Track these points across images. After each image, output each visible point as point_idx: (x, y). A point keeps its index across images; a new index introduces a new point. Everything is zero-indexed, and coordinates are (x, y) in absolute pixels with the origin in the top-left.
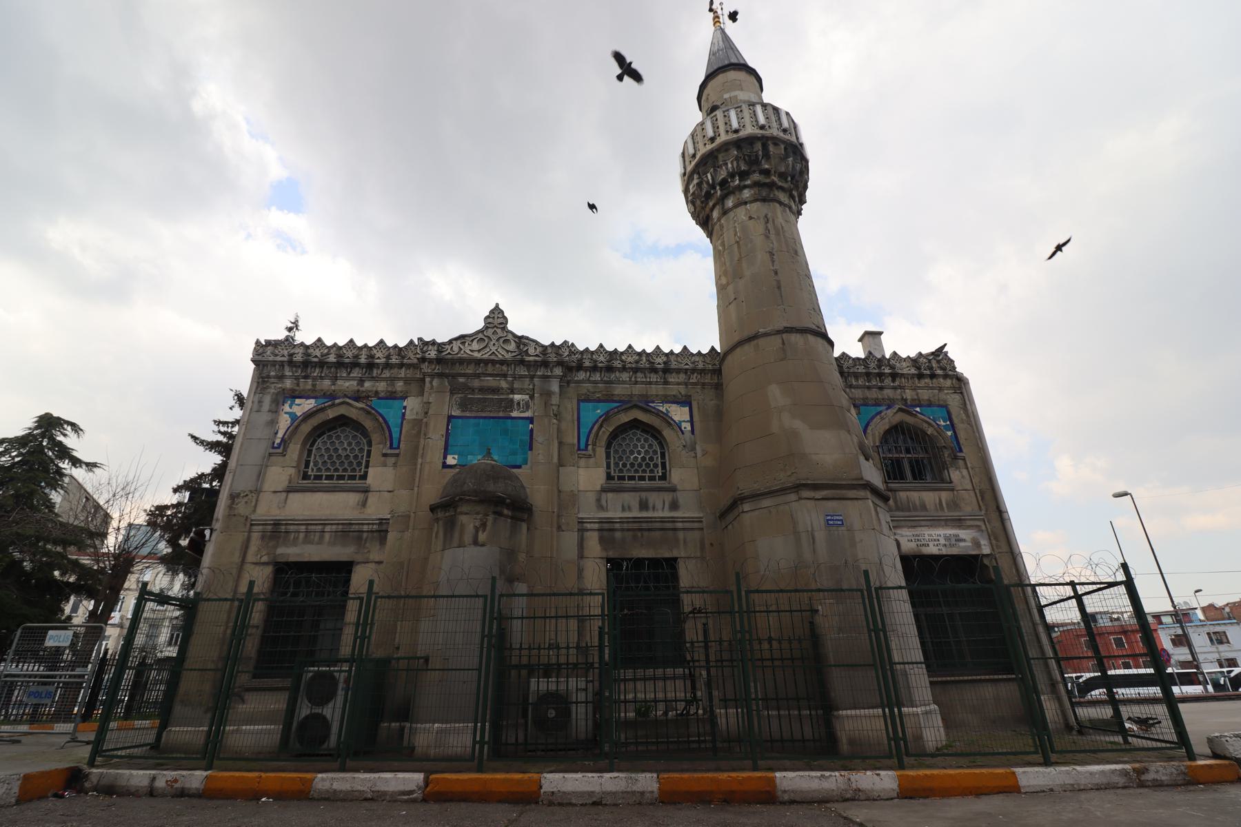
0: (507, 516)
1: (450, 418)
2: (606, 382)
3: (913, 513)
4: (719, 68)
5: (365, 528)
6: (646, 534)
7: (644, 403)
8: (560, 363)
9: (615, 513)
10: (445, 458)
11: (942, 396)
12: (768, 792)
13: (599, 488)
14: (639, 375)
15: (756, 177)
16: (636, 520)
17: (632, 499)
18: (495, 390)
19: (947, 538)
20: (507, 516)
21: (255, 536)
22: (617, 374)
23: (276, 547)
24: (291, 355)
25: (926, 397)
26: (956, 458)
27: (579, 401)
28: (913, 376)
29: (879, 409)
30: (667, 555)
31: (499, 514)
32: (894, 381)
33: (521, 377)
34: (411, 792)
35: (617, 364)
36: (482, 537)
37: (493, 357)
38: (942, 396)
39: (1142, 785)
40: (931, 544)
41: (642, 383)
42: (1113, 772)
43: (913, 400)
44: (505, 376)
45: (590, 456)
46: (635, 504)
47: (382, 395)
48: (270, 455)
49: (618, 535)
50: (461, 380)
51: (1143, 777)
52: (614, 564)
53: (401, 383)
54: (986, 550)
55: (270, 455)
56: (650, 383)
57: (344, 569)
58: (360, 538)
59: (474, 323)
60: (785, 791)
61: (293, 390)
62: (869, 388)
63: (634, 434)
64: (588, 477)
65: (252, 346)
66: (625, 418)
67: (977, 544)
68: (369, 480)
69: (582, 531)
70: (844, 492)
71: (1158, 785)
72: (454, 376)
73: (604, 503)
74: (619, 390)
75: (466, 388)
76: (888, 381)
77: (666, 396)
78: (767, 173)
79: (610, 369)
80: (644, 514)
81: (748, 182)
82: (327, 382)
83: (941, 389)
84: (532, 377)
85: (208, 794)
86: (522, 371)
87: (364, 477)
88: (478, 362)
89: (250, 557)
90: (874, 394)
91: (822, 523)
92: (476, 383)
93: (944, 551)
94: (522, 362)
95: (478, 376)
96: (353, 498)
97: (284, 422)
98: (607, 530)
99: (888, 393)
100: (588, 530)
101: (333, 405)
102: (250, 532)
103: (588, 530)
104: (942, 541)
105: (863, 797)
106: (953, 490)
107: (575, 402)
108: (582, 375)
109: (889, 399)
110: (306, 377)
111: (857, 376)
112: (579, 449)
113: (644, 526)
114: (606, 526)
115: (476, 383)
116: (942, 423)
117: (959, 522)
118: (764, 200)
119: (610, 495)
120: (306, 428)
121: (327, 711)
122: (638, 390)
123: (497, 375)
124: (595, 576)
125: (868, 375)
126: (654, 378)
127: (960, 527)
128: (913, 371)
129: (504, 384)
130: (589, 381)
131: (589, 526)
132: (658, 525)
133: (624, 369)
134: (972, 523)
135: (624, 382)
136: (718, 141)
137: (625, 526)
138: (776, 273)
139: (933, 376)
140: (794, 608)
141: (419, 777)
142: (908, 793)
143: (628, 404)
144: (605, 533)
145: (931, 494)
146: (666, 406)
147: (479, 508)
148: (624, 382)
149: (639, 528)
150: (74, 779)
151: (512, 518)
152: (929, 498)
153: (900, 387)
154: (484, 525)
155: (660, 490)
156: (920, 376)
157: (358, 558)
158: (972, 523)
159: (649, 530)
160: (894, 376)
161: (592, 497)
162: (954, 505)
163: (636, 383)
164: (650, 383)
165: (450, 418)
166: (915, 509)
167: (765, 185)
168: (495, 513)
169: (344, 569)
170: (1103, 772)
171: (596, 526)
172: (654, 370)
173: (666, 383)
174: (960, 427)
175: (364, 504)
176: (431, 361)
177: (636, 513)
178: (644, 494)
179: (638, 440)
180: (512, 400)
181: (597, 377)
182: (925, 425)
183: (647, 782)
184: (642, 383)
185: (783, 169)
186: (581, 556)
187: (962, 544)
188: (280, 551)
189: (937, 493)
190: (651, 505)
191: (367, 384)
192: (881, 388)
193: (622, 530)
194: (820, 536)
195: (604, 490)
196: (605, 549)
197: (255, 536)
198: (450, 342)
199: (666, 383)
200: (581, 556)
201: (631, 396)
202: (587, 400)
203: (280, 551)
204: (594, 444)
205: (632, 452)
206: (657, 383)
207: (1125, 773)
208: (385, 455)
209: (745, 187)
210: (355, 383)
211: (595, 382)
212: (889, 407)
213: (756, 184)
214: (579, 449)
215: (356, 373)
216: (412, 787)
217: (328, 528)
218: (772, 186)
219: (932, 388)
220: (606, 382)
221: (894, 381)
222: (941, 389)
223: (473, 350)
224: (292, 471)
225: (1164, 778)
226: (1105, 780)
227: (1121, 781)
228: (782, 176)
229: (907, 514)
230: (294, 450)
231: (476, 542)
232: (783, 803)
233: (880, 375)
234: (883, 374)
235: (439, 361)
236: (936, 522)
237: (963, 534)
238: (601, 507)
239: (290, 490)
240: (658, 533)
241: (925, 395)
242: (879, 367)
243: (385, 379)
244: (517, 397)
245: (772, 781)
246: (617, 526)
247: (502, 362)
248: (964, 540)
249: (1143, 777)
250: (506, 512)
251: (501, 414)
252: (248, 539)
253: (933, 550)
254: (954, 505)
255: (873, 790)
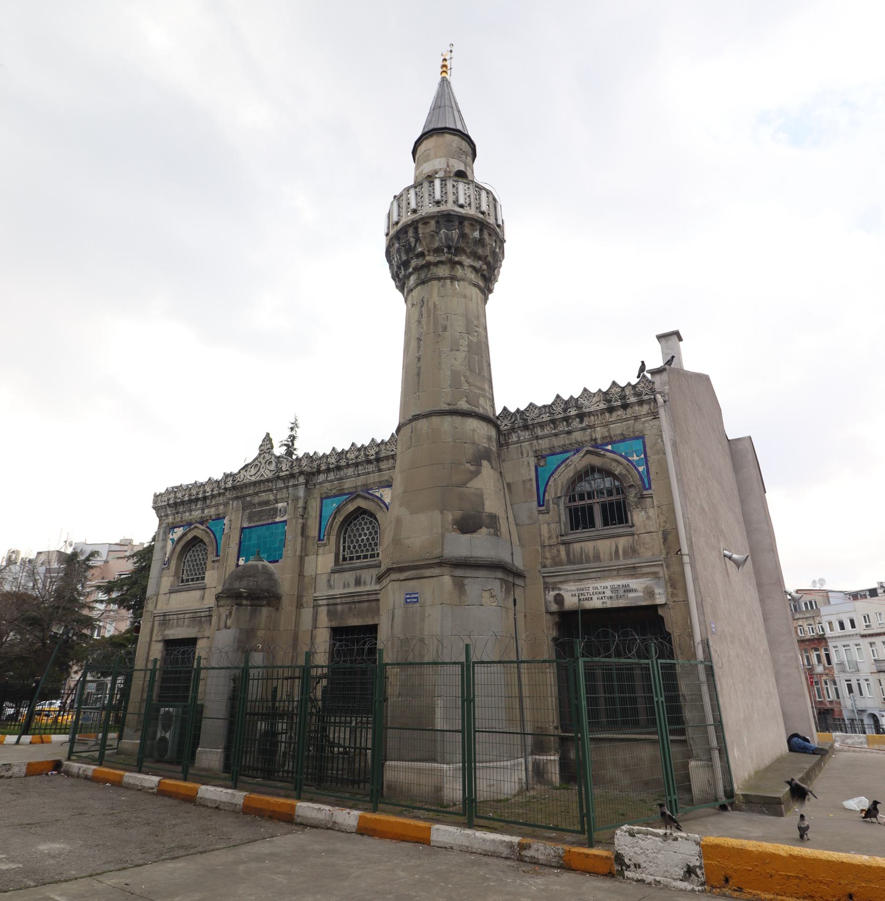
0: (247, 605)
1: (242, 529)
2: (339, 479)
3: (552, 569)
4: (416, 143)
5: (203, 614)
6: (358, 605)
7: (365, 492)
8: (301, 473)
9: (338, 591)
10: (238, 560)
11: (639, 426)
12: (291, 815)
13: (329, 571)
14: (360, 468)
15: (414, 263)
16: (351, 595)
17: (350, 577)
18: (267, 503)
19: (614, 590)
20: (247, 605)
21: (156, 623)
22: (345, 471)
23: (164, 630)
24: (168, 500)
25: (618, 432)
26: (642, 497)
27: (322, 499)
28: (602, 412)
29: (566, 455)
30: (371, 623)
31: (239, 605)
32: (581, 422)
33: (281, 489)
34: (152, 788)
35: (343, 463)
36: (229, 622)
37: (262, 478)
38: (639, 426)
39: (521, 859)
40: (595, 597)
41: (364, 474)
42: (502, 842)
43: (603, 438)
44: (271, 490)
45: (325, 545)
46: (352, 582)
47: (213, 517)
48: (163, 569)
49: (339, 608)
50: (248, 499)
51: (524, 853)
52: (337, 632)
53: (222, 507)
54: (660, 600)
55: (163, 569)
56: (369, 473)
57: (193, 642)
58: (200, 621)
59: (252, 453)
60: (298, 816)
61: (173, 523)
62: (556, 435)
63: (363, 519)
64: (322, 562)
65: (152, 497)
66: (351, 507)
67: (650, 593)
68: (206, 581)
69: (316, 607)
70: (423, 571)
71: (535, 862)
72: (244, 497)
73: (332, 583)
74: (348, 484)
75: (251, 505)
76: (576, 424)
77: (380, 482)
78: (422, 255)
79: (339, 468)
80: (359, 589)
81: (411, 270)
82: (187, 514)
83: (636, 418)
84: (287, 487)
85: (94, 779)
86: (280, 484)
87: (203, 578)
88: (255, 483)
89: (154, 638)
90: (563, 440)
91: (403, 601)
92: (256, 500)
93: (609, 604)
94: (279, 477)
95: (256, 494)
96: (197, 594)
97: (169, 546)
98: (332, 603)
99: (577, 436)
100: (320, 606)
101: (190, 530)
102: (154, 621)
103: (320, 606)
104: (608, 593)
105: (337, 828)
106: (633, 535)
107: (319, 500)
108: (322, 477)
109: (577, 442)
110: (177, 513)
111: (542, 425)
112: (319, 540)
113: (356, 599)
114: (331, 601)
115: (256, 500)
116: (635, 458)
117: (633, 571)
118: (423, 283)
119: (336, 575)
120: (179, 548)
121: (168, 735)
122: (361, 481)
123: (267, 491)
124: (323, 639)
125: (553, 421)
126: (371, 468)
127: (633, 576)
128: (602, 406)
129: (272, 497)
130: (327, 481)
131: (320, 602)
132: (365, 598)
133: (348, 466)
134: (648, 570)
135: (350, 477)
136: (443, 208)
137: (344, 600)
138: (419, 359)
139: (625, 406)
140: (523, 658)
141: (156, 779)
142: (363, 830)
143: (354, 495)
144: (331, 607)
145: (607, 542)
146: (381, 490)
147: (229, 602)
148: (350, 477)
149: (353, 601)
150: (57, 765)
151: (251, 605)
152: (605, 546)
153: (590, 427)
154: (230, 613)
155: (369, 567)
156: (611, 410)
157: (199, 635)
158: (648, 570)
159: (360, 602)
160: (581, 416)
161: (324, 578)
162: (633, 551)
163: (359, 475)
164: (369, 473)
165: (242, 529)
166: (588, 561)
167: (423, 267)
168: (236, 604)
169: (193, 642)
170: (493, 841)
171: (325, 602)
172: (369, 462)
173: (380, 470)
174: (652, 458)
175: (203, 598)
176: (230, 489)
177: (353, 589)
178: (358, 572)
179: (366, 524)
180: (277, 508)
181: (331, 476)
182: (614, 464)
183: (238, 797)
184: (364, 474)
185: (436, 245)
186: (315, 627)
187: (631, 595)
188: (167, 632)
189: (613, 541)
190: (363, 581)
191: (206, 511)
192: (569, 433)
193: (342, 604)
194: (399, 613)
195: (333, 572)
196: (330, 620)
197: (156, 623)
198: (239, 472)
199: (380, 470)
200: (315, 627)
201: (356, 487)
202: (328, 497)
203: (167, 632)
204: (329, 534)
205: (360, 535)
206: (373, 472)
207: (510, 845)
208: (213, 562)
209: (411, 274)
210: (200, 512)
211: (331, 481)
212: (578, 451)
213: (417, 269)
214: (319, 540)
215: (200, 505)
216: (153, 785)
217: (187, 616)
218: (428, 265)
219: (627, 420)
220: (339, 479)
221: (581, 422)
222: (636, 418)
223: (251, 476)
224: (172, 578)
225: (541, 857)
226: (492, 849)
227: (505, 852)
228: (438, 251)
229: (575, 567)
230: (173, 563)
231: (226, 627)
232: (297, 824)
233: (566, 419)
234: (570, 417)
235: (234, 488)
236: (606, 573)
237: (633, 583)
238: (330, 587)
239: (171, 592)
240: (365, 605)
241: (617, 429)
242: (565, 410)
243: (214, 506)
244: (280, 505)
245: (293, 807)
246: (338, 601)
247: (268, 480)
248: (635, 591)
249: (524, 853)
250: (245, 602)
251: (270, 521)
252: (153, 625)
253: (596, 603)
254: (633, 551)
255: (342, 824)
